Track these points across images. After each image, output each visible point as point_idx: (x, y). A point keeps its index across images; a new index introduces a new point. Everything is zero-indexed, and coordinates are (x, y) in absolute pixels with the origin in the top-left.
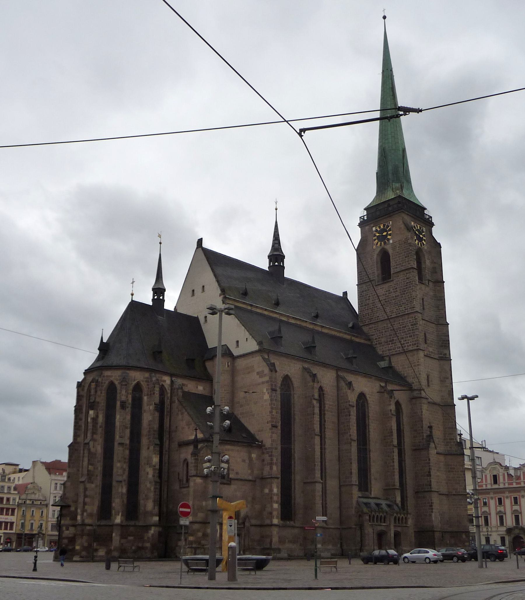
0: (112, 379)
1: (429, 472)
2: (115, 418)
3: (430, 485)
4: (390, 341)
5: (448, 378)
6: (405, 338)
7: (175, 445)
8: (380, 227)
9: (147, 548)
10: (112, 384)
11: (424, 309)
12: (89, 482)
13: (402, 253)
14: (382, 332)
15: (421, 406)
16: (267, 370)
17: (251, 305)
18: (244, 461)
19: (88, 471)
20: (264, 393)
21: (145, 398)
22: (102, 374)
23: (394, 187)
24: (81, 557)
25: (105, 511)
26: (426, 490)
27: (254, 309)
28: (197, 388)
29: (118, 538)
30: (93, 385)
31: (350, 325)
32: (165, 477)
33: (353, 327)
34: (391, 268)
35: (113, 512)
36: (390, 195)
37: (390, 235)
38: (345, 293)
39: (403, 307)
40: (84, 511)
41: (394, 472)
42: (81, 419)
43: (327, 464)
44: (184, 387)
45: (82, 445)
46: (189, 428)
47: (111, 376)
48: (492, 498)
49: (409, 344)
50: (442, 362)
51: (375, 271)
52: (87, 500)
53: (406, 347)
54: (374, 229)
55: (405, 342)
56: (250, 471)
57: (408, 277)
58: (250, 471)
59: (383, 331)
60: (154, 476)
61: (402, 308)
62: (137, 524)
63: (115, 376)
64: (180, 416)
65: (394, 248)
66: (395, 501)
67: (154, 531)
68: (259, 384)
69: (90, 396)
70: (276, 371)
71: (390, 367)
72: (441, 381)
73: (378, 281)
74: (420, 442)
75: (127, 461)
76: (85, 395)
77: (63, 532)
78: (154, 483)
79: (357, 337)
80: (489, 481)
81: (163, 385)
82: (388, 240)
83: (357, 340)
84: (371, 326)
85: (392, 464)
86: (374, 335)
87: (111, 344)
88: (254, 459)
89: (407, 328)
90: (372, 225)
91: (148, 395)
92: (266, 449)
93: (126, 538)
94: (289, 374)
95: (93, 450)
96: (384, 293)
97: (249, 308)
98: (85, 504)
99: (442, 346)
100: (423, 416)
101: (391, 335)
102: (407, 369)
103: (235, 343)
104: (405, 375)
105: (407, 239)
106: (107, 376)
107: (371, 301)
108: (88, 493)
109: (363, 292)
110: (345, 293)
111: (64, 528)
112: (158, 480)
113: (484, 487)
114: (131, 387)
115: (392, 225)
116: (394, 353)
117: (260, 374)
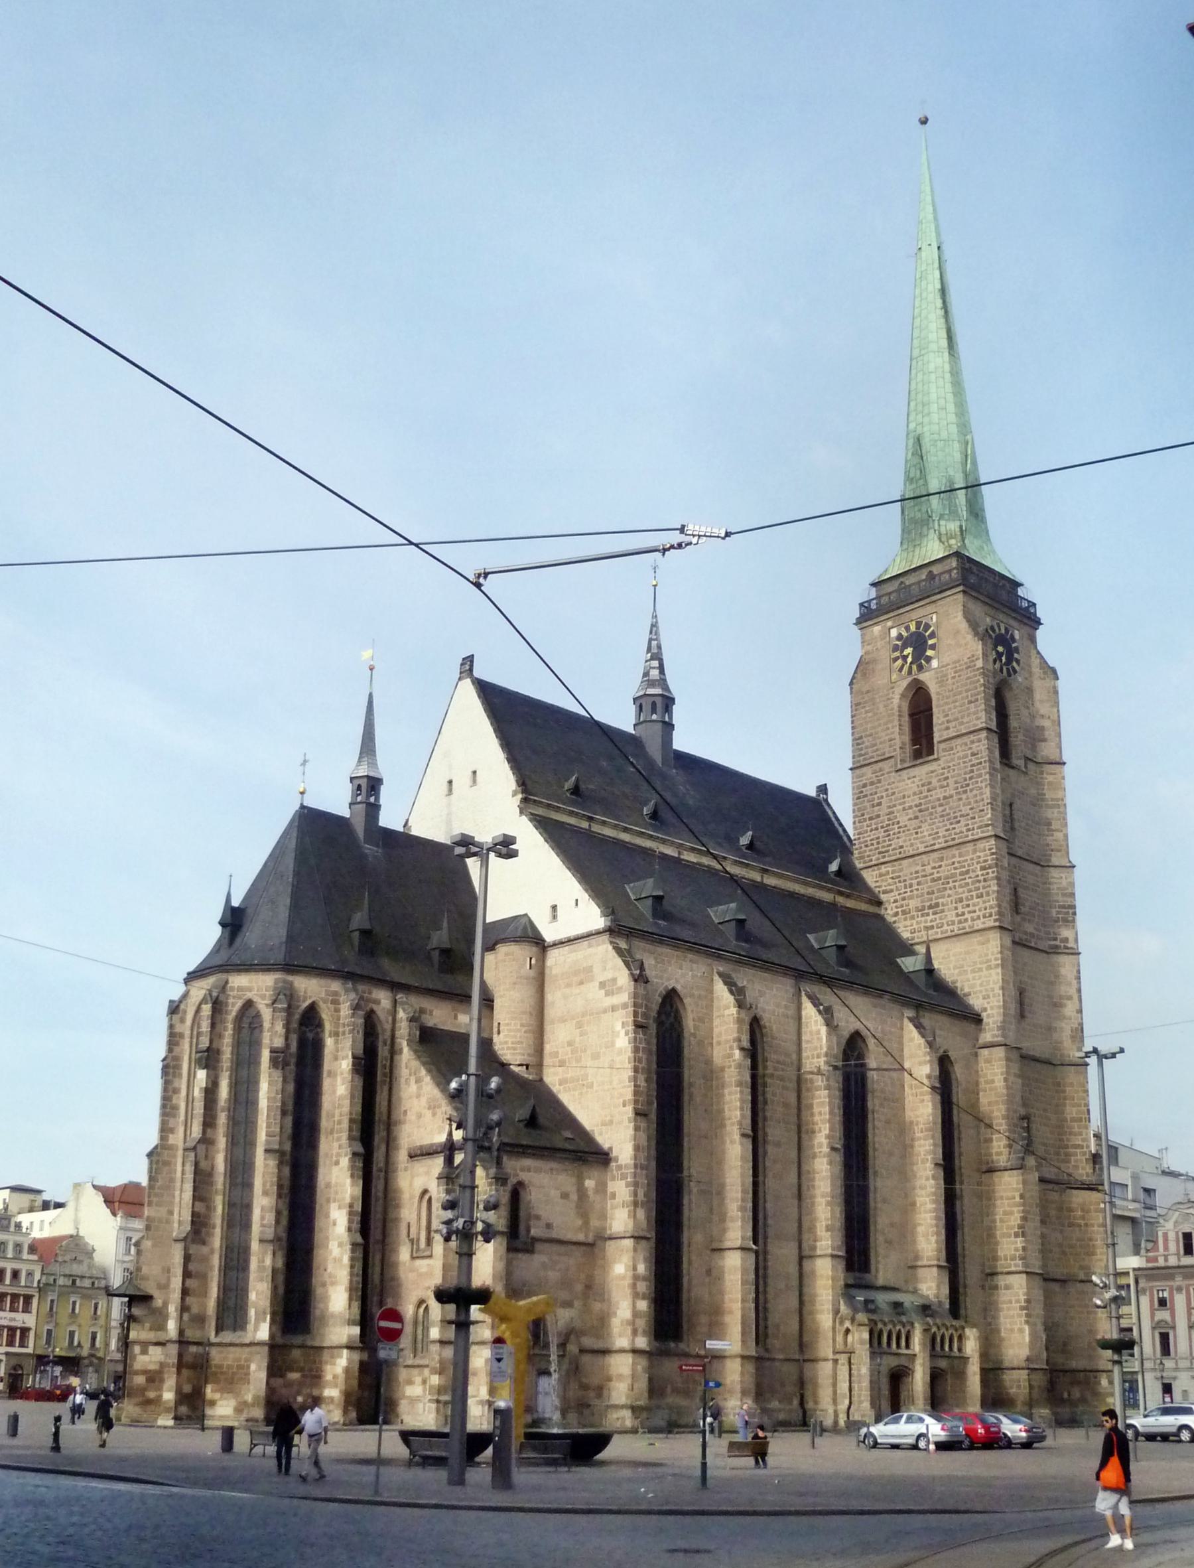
0: (249, 995)
2: (257, 1091)
4: (930, 907)
6: (968, 899)
7: (402, 1156)
8: (908, 628)
9: (332, 1399)
10: (249, 1004)
11: (1013, 829)
12: (193, 1242)
13: (960, 693)
14: (911, 886)
16: (623, 977)
17: (590, 819)
18: (565, 1196)
19: (194, 1214)
20: (615, 1035)
21: (329, 1042)
22: (227, 982)
23: (943, 530)
24: (176, 1418)
25: (232, 1312)
26: (1013, 1269)
27: (596, 828)
28: (456, 1017)
29: (263, 1375)
30: (207, 1009)
31: (834, 867)
32: (375, 1234)
33: (839, 873)
34: (935, 729)
35: (252, 1313)
36: (933, 549)
37: (933, 647)
38: (823, 789)
39: (963, 823)
40: (184, 1308)
42: (176, 1091)
43: (769, 1205)
44: (423, 1016)
45: (180, 1152)
46: (434, 1114)
47: (250, 990)
48: (1179, 1289)
51: (894, 733)
52: (189, 1282)
53: (970, 923)
54: (894, 633)
55: (966, 910)
56: (579, 1222)
57: (975, 750)
58: (579, 1222)
59: (914, 882)
60: (349, 1230)
61: (960, 827)
62: (309, 1343)
63: (256, 987)
64: (413, 1088)
65: (941, 681)
67: (349, 1360)
68: (605, 1011)
69: (199, 1034)
70: (647, 982)
71: (930, 971)
73: (902, 761)
75: (286, 1191)
76: (187, 1033)
77: (134, 1357)
78: (349, 1247)
79: (848, 896)
80: (1172, 1247)
81: (372, 1011)
82: (928, 659)
83: (850, 903)
84: (883, 869)
86: (892, 891)
87: (250, 911)
88: (590, 1193)
89: (972, 875)
90: (889, 624)
91: (336, 1034)
92: (619, 1167)
93: (282, 1376)
94: (679, 987)
95: (203, 1165)
96: (916, 790)
97: (585, 825)
98: (185, 1292)
101: (933, 893)
102: (970, 976)
103: (549, 911)
104: (966, 990)
105: (972, 659)
106: (240, 989)
107: (884, 810)
108: (191, 1267)
109: (865, 786)
110: (823, 789)
111: (137, 1349)
112: (360, 1240)
113: (1161, 1262)
114: (297, 1016)
115: (938, 625)
116: (939, 936)
117: (608, 987)
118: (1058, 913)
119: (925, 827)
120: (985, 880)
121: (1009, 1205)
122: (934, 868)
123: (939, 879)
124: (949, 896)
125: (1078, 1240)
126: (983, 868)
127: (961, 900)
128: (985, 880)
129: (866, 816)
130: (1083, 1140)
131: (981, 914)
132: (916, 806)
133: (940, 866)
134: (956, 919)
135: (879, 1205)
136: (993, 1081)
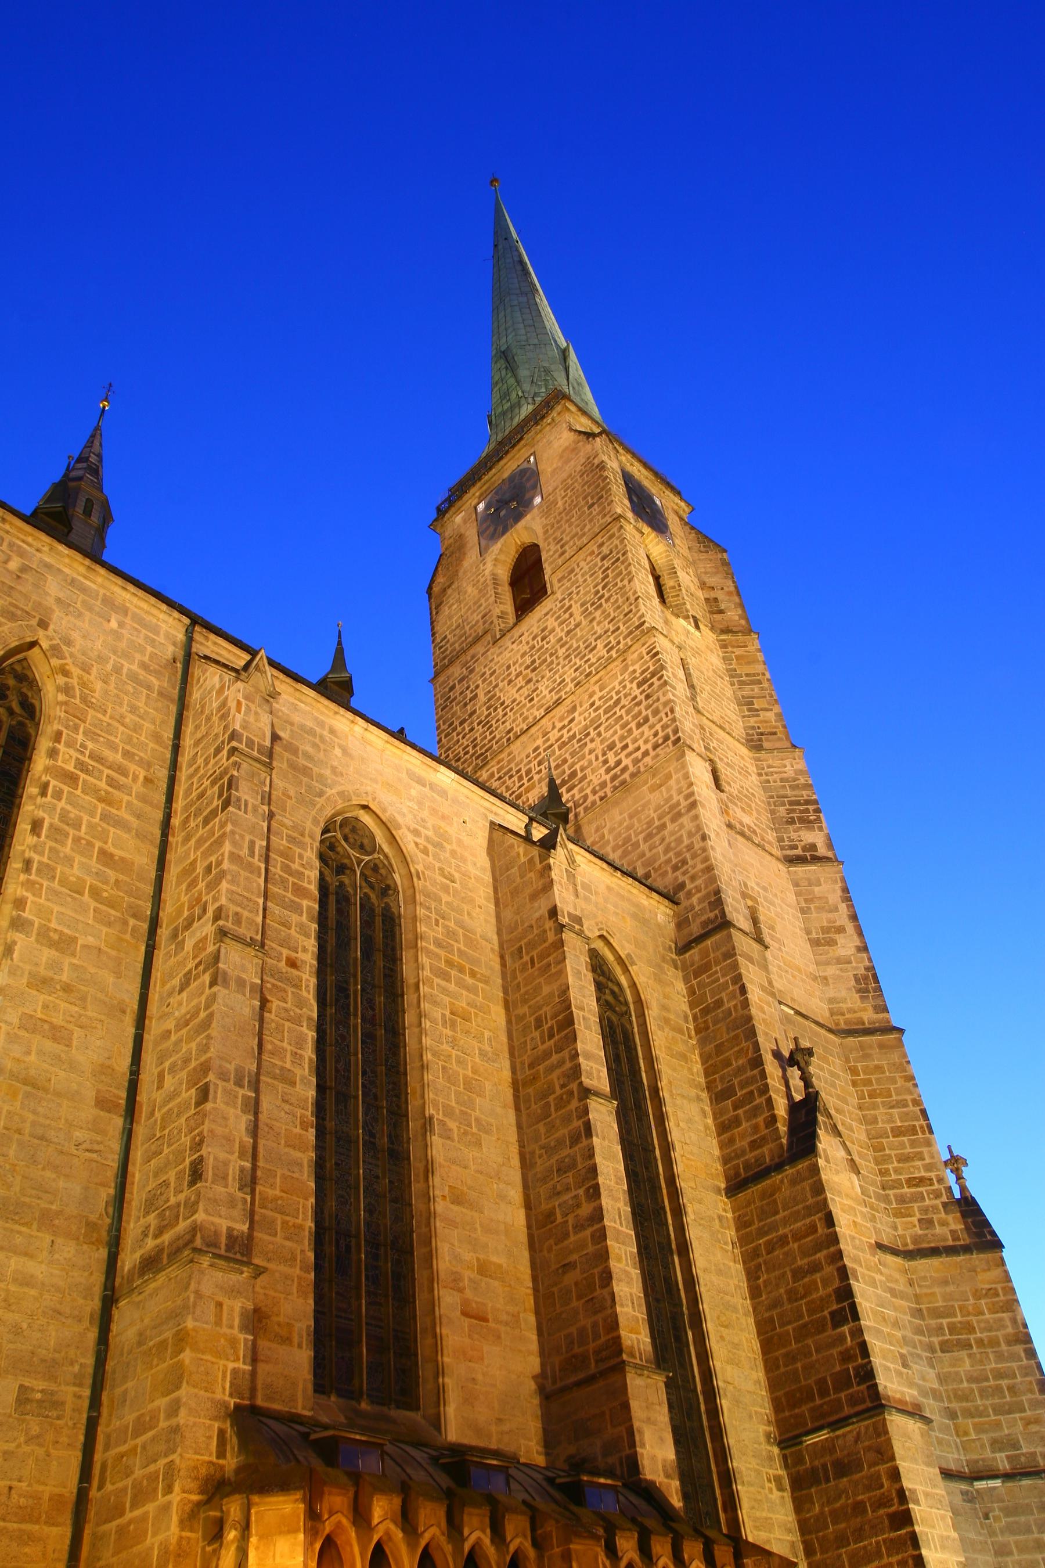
1: (846, 1294)
3: (868, 1374)
5: (841, 930)
15: (735, 966)
41: (604, 1255)
49: (639, 754)
50: (800, 870)
55: (622, 756)
66: (633, 1464)
72: (815, 943)
74: (754, 1145)
85: (586, 1209)
89: (623, 702)
99: (792, 822)
100: (754, 1011)
101: (565, 761)
118: (789, 811)
119: (541, 687)
120: (648, 697)
121: (804, 1254)
122: (560, 730)
123: (574, 736)
124: (591, 752)
125: (971, 1379)
126: (639, 685)
127: (611, 747)
128: (648, 697)
129: (456, 723)
130: (929, 1168)
131: (649, 746)
132: (527, 667)
133: (572, 720)
134: (608, 777)
135: (440, 1207)
136: (719, 1003)
